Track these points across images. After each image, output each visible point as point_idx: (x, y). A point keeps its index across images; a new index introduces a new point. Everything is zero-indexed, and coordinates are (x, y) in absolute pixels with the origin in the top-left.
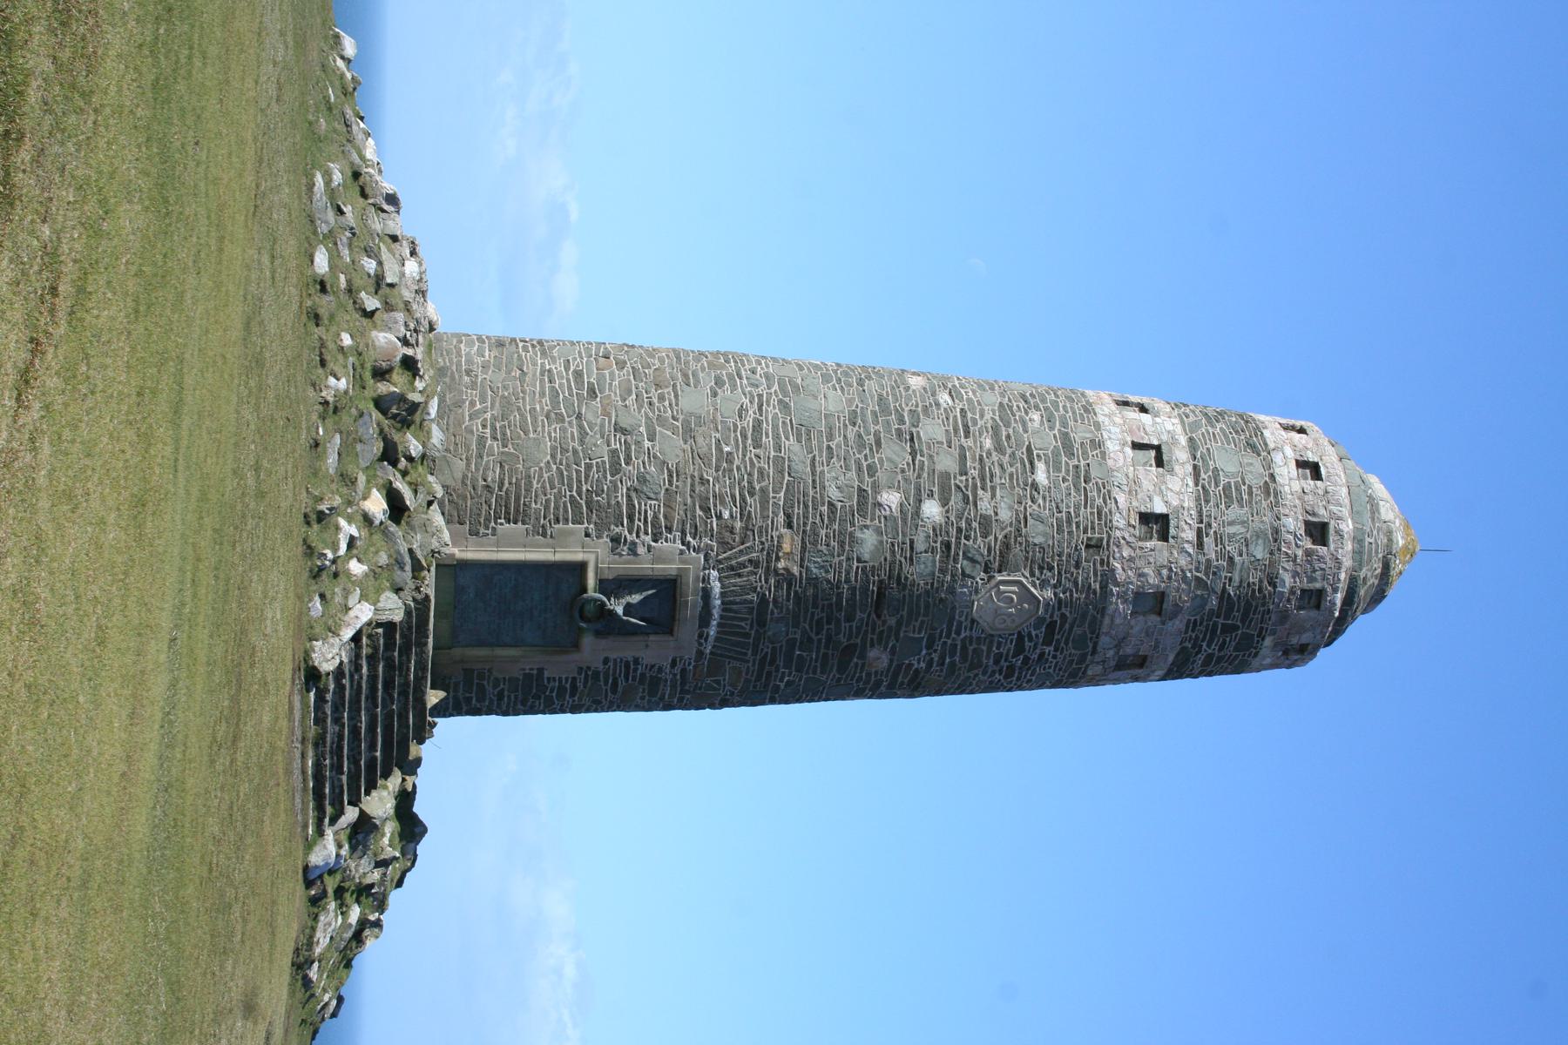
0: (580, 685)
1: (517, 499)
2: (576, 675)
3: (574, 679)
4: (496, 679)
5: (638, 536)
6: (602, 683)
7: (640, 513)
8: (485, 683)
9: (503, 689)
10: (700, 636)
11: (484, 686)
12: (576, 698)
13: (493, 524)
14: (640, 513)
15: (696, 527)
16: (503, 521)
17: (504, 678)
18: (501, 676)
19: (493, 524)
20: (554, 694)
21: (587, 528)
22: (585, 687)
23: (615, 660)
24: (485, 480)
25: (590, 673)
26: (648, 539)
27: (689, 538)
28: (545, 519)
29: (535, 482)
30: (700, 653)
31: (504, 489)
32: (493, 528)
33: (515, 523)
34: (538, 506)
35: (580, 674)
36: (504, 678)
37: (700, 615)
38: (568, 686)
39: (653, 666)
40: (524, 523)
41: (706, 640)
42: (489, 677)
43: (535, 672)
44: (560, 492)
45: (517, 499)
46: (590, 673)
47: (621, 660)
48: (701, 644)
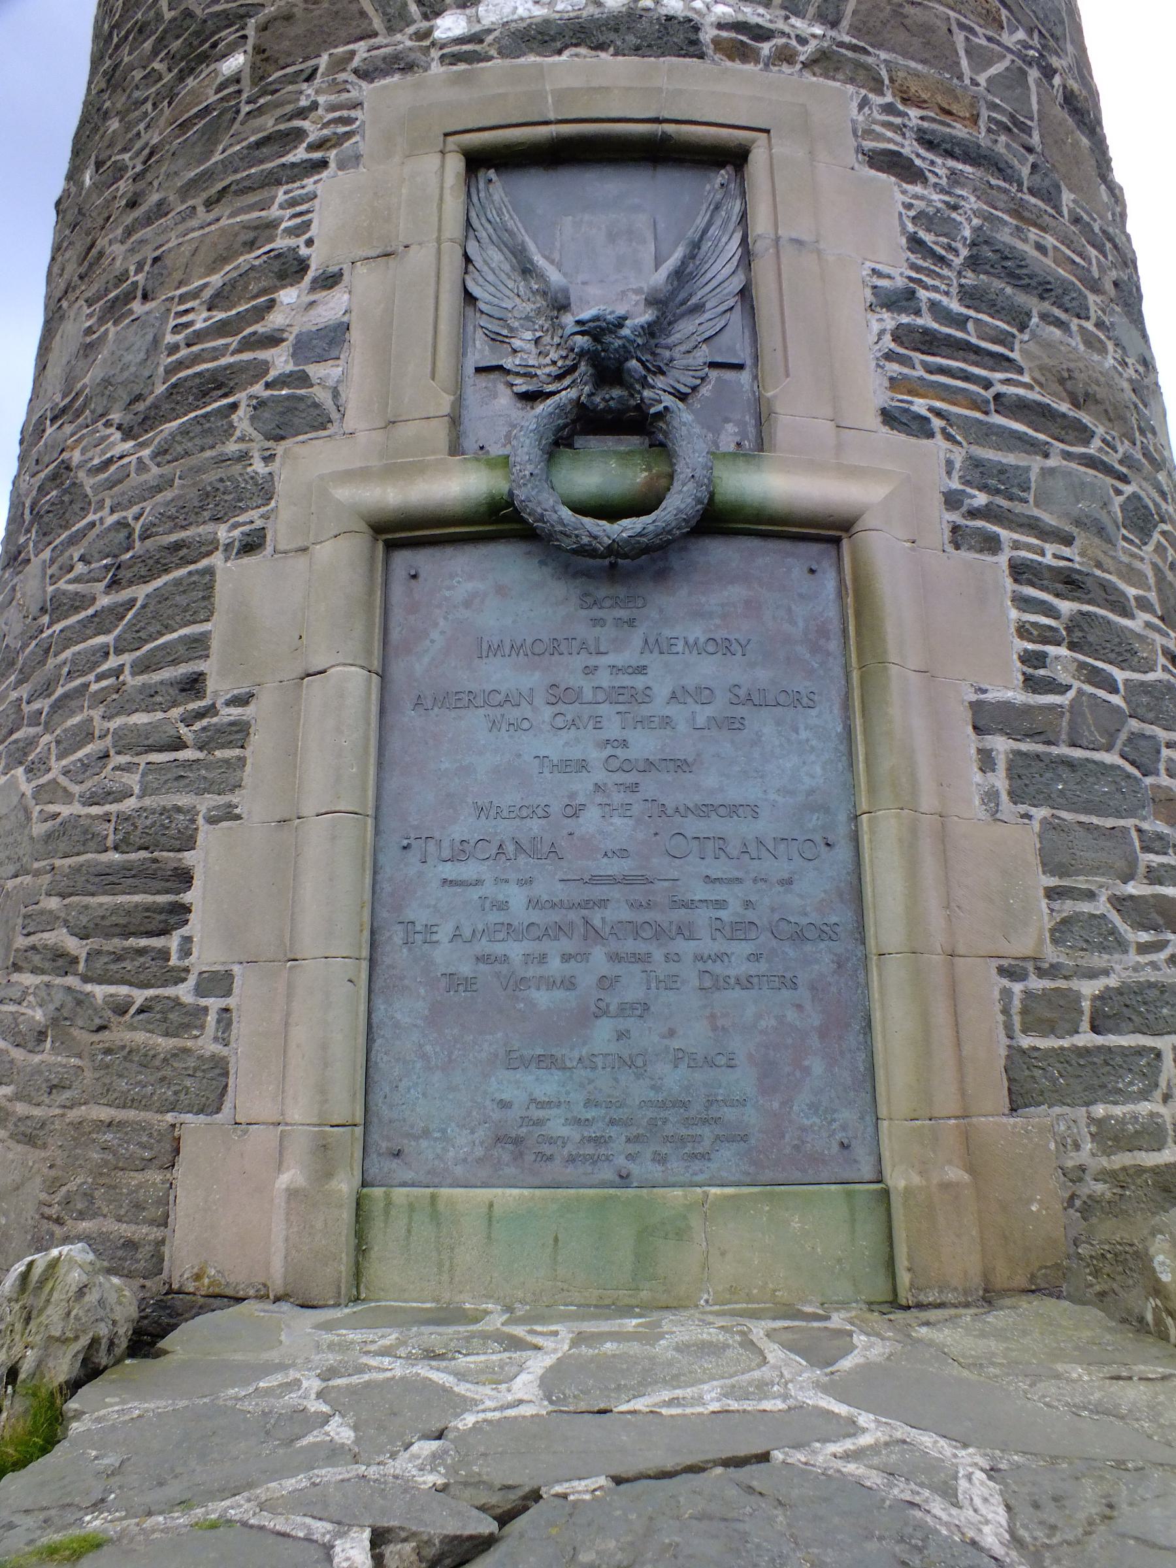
0: (1050, 555)
1: (109, 880)
2: (1003, 559)
3: (1019, 571)
4: (1062, 930)
5: (273, 340)
6: (1036, 464)
7: (196, 359)
8: (1089, 989)
9: (1119, 902)
10: (741, 53)
11: (1101, 998)
12: (1131, 592)
13: (184, 992)
14: (196, 359)
15: (259, 144)
16: (173, 942)
17: (1052, 894)
18: (1043, 914)
19: (184, 992)
20: (1120, 675)
21: (228, 547)
22: (1068, 541)
23: (894, 383)
24: (41, 1036)
25: (981, 499)
26: (288, 296)
27: (300, 154)
28: (178, 744)
29: (65, 811)
30: (824, 62)
31: (72, 945)
32: (200, 991)
33: (185, 878)
34: (133, 780)
35: (991, 544)
36: (1052, 894)
37: (637, 50)
38: (1066, 607)
39: (915, 243)
40: (188, 842)
41: (761, 34)
42: (1053, 971)
43: (1001, 745)
44: (100, 699)
45: (109, 880)
46: (981, 499)
47: (890, 356)
48: (785, 56)
